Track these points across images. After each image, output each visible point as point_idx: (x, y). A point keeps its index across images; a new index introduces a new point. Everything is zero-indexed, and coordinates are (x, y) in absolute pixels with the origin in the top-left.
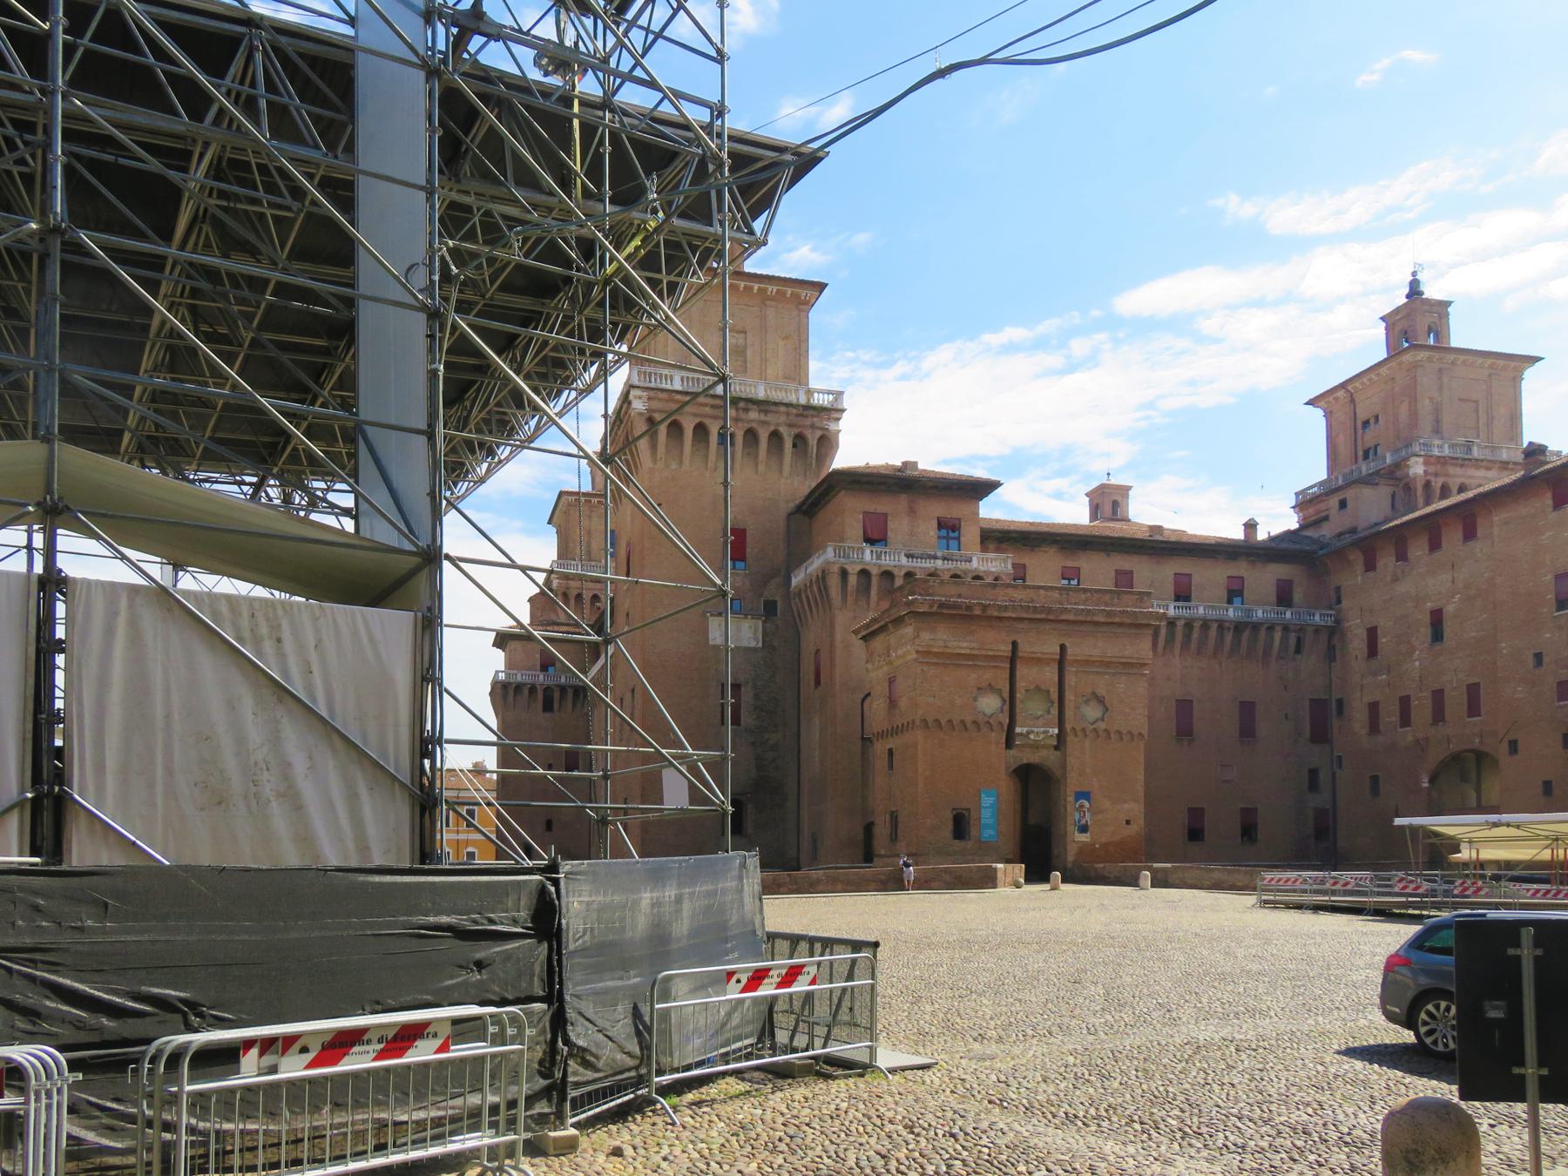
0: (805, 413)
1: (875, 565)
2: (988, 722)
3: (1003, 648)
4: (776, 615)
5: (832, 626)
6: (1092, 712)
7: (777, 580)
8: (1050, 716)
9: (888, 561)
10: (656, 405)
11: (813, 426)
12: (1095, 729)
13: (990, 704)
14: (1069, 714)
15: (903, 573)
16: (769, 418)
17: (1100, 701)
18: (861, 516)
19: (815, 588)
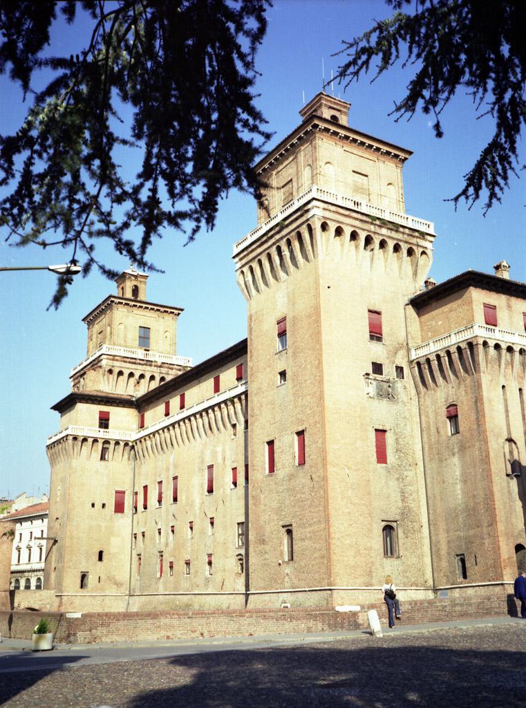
5: (478, 386)
10: (328, 214)
11: (418, 246)
15: (518, 350)
16: (394, 234)
19: (455, 356)
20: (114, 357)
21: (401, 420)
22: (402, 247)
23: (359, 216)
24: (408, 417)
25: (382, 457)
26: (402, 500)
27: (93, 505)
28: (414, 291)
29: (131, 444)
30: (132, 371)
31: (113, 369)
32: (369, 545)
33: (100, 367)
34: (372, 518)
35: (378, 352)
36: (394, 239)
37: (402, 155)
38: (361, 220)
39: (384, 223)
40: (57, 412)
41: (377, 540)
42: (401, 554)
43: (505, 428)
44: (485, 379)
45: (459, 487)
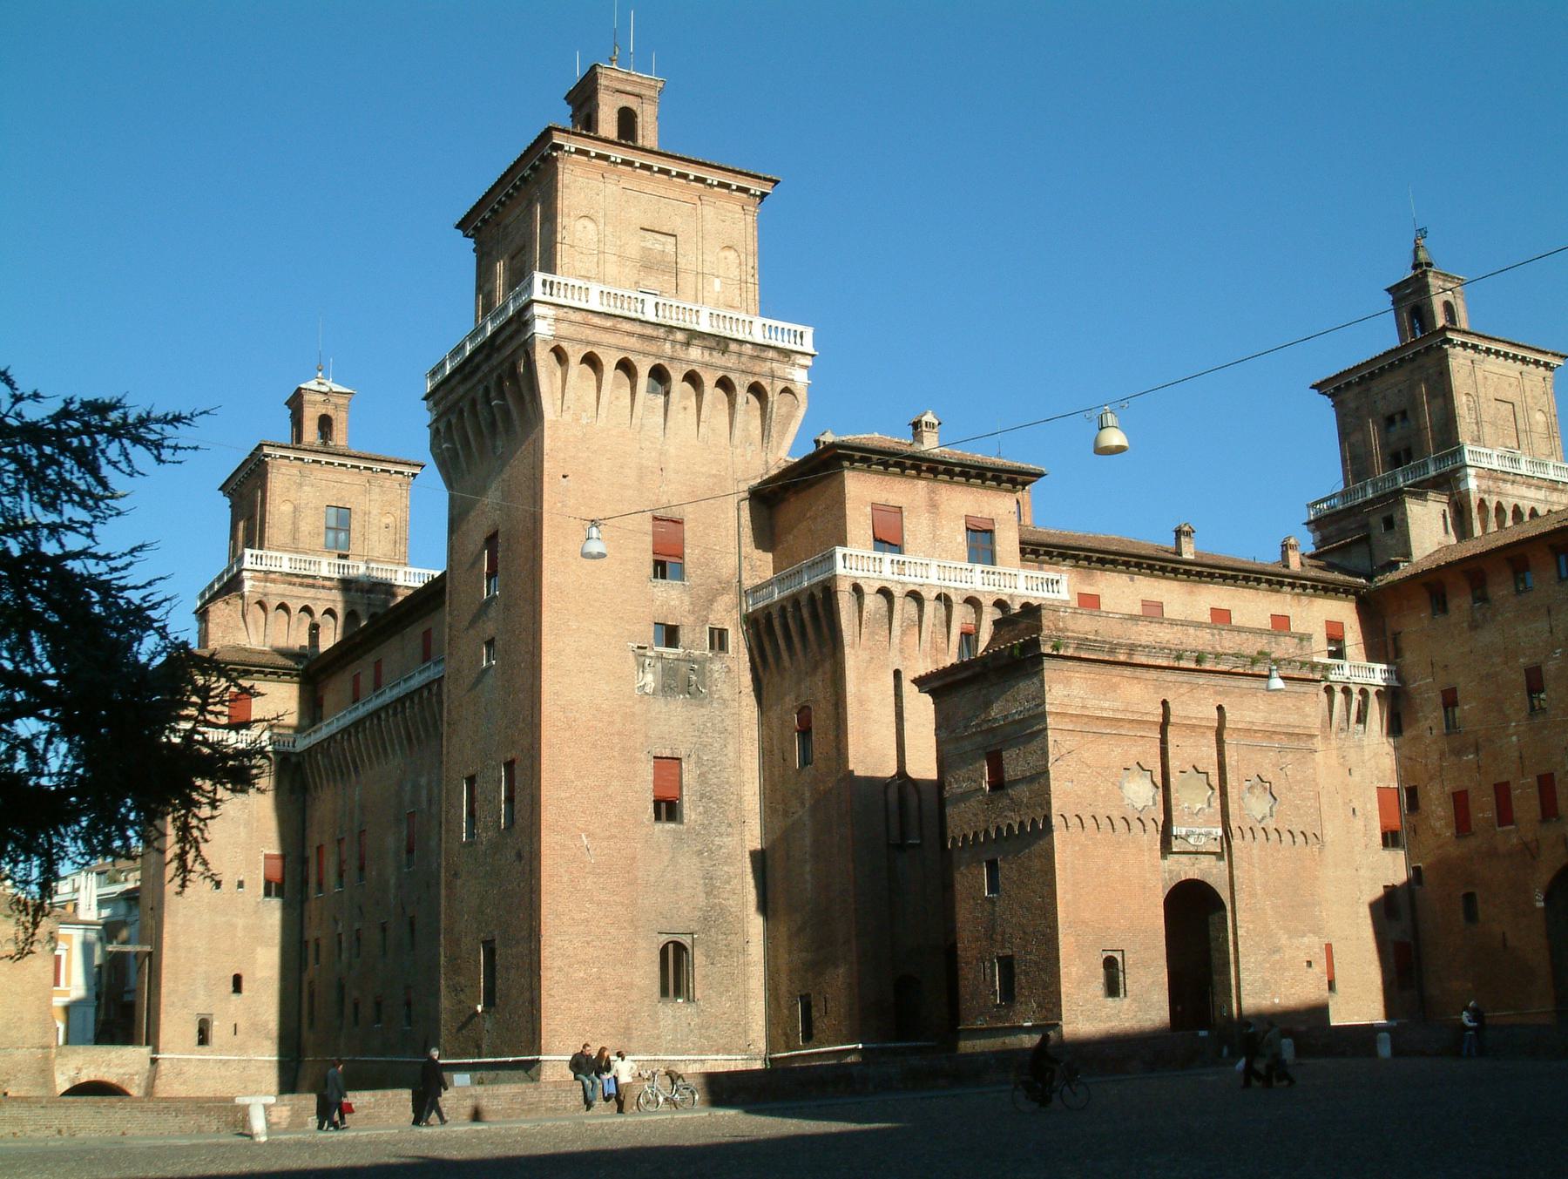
0: (763, 355)
1: (898, 582)
8: (1212, 810)
9: (912, 580)
10: (565, 329)
13: (1141, 793)
15: (934, 595)
16: (717, 358)
18: (869, 509)
19: (805, 613)
21: (716, 735)
22: (736, 383)
23: (638, 329)
24: (730, 728)
25: (667, 809)
26: (707, 893)
28: (763, 472)
29: (294, 759)
31: (265, 599)
32: (626, 979)
34: (636, 928)
35: (670, 599)
36: (717, 368)
37: (756, 187)
39: (693, 336)
41: (647, 973)
44: (854, 660)
45: (808, 868)
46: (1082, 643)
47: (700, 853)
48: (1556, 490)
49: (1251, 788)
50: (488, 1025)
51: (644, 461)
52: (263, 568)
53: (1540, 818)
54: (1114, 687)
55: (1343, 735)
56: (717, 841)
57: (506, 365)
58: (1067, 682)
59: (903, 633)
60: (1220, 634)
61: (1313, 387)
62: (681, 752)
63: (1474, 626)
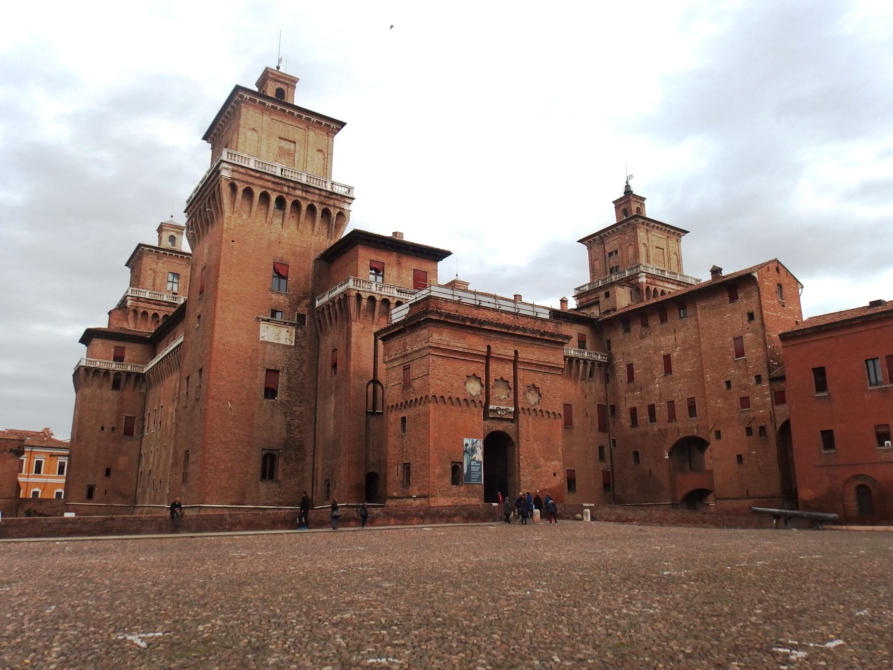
1: (378, 294)
2: (473, 400)
3: (482, 350)
4: (305, 325)
6: (533, 398)
7: (306, 301)
8: (510, 399)
10: (236, 175)
11: (334, 206)
12: (534, 409)
13: (474, 388)
14: (520, 398)
15: (395, 301)
16: (308, 196)
17: (536, 391)
18: (369, 262)
20: (138, 299)
22: (317, 208)
27: (103, 428)
30: (156, 311)
31: (137, 309)
32: (245, 470)
33: (126, 307)
38: (273, 182)
40: (84, 346)
41: (254, 466)
42: (280, 478)
43: (372, 370)
44: (356, 327)
46: (448, 316)
47: (285, 413)
48: (680, 285)
49: (529, 391)
50: (183, 490)
51: (271, 238)
52: (137, 295)
53: (668, 420)
54: (464, 338)
55: (583, 382)
56: (294, 408)
57: (212, 192)
58: (440, 333)
59: (380, 317)
60: (518, 318)
61: (580, 241)
62: (279, 367)
63: (642, 338)
